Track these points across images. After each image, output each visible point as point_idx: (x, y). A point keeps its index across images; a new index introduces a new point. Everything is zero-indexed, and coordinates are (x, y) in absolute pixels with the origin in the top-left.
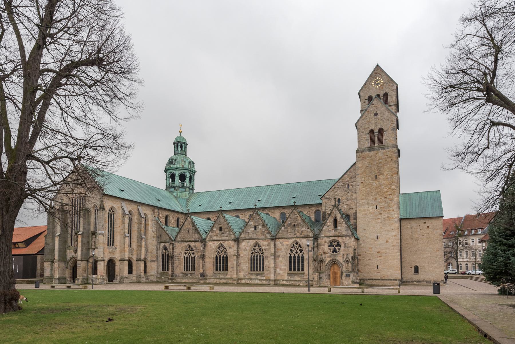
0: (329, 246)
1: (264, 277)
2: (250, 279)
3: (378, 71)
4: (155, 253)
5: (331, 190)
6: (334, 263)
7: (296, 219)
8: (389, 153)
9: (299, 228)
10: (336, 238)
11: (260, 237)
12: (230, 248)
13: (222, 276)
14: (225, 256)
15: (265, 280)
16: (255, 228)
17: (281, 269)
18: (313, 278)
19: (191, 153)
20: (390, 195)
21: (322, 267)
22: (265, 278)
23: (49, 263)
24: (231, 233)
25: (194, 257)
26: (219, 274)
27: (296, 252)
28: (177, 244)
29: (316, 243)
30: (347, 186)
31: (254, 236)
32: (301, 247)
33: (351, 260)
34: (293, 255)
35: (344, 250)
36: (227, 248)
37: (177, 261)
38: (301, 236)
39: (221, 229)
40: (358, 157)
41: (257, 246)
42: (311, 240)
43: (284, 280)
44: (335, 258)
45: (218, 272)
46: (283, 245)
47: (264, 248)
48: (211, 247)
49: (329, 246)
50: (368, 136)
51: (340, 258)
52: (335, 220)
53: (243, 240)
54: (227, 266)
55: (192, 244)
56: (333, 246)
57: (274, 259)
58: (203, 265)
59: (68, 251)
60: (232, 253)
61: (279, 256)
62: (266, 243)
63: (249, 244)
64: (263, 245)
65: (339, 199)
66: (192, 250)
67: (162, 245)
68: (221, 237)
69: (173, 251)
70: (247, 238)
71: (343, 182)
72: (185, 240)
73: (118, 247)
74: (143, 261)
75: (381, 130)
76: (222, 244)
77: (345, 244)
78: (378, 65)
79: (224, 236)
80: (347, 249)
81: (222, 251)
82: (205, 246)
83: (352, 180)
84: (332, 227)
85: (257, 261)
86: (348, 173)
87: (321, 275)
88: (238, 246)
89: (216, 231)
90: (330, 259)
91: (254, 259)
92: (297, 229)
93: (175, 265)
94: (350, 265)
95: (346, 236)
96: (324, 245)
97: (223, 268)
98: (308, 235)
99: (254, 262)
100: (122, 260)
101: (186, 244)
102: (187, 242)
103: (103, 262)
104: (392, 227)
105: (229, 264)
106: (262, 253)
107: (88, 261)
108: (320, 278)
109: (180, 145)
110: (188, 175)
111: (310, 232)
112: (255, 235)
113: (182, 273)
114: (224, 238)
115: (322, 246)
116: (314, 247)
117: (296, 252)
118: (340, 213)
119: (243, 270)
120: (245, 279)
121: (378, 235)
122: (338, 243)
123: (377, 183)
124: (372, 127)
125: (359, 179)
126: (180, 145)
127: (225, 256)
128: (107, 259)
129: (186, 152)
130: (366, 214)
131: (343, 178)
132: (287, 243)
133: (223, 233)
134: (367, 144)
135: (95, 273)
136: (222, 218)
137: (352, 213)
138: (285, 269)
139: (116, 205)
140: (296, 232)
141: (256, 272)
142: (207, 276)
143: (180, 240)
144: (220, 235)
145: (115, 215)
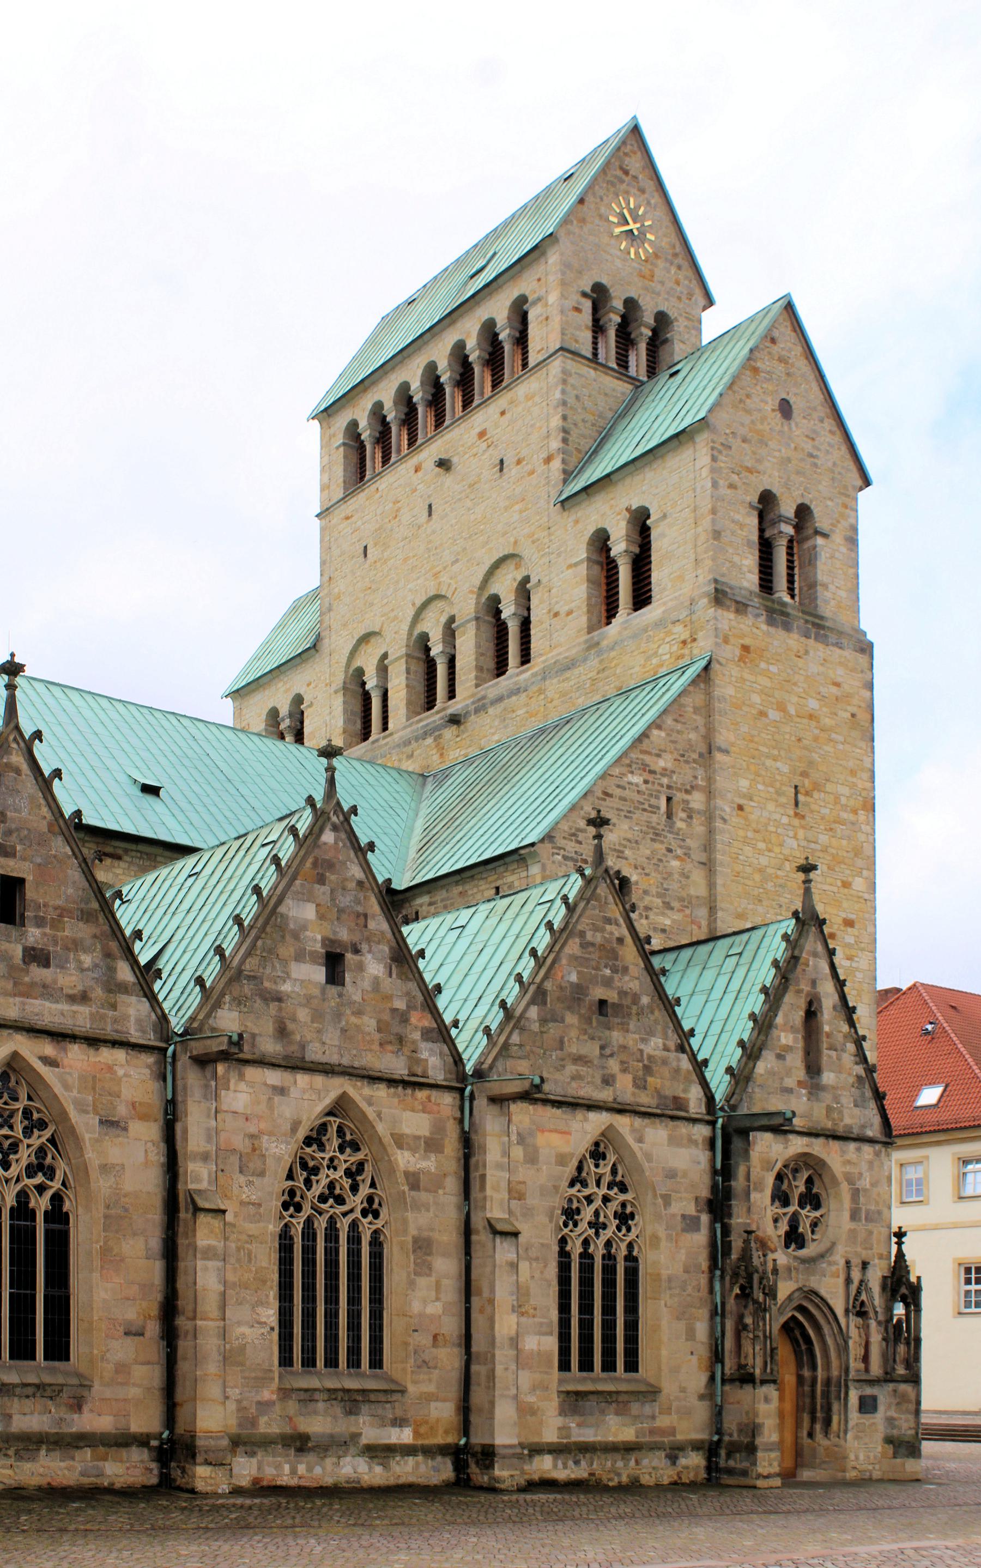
1: (399, 1422)
2: (300, 1443)
10: (817, 1147)
14: (41, 1204)
15: (409, 1450)
22: (405, 1436)
32: (623, 1188)
33: (877, 1302)
34: (575, 1248)
36: (84, 1124)
38: (646, 1100)
42: (692, 1142)
43: (536, 1450)
44: (814, 1282)
46: (532, 1159)
47: (404, 1160)
63: (286, 1110)
64: (400, 1141)
68: (27, 991)
70: (269, 1047)
71: (645, 768)
77: (856, 1193)
80: (861, 1227)
91: (309, 1252)
92: (616, 1036)
99: (309, 1288)
106: (371, 1210)
112: (332, 1036)
117: (597, 1225)
120: (241, 1442)
123: (801, 833)
127: (41, 1204)
132: (555, 1139)
140: (613, 1065)
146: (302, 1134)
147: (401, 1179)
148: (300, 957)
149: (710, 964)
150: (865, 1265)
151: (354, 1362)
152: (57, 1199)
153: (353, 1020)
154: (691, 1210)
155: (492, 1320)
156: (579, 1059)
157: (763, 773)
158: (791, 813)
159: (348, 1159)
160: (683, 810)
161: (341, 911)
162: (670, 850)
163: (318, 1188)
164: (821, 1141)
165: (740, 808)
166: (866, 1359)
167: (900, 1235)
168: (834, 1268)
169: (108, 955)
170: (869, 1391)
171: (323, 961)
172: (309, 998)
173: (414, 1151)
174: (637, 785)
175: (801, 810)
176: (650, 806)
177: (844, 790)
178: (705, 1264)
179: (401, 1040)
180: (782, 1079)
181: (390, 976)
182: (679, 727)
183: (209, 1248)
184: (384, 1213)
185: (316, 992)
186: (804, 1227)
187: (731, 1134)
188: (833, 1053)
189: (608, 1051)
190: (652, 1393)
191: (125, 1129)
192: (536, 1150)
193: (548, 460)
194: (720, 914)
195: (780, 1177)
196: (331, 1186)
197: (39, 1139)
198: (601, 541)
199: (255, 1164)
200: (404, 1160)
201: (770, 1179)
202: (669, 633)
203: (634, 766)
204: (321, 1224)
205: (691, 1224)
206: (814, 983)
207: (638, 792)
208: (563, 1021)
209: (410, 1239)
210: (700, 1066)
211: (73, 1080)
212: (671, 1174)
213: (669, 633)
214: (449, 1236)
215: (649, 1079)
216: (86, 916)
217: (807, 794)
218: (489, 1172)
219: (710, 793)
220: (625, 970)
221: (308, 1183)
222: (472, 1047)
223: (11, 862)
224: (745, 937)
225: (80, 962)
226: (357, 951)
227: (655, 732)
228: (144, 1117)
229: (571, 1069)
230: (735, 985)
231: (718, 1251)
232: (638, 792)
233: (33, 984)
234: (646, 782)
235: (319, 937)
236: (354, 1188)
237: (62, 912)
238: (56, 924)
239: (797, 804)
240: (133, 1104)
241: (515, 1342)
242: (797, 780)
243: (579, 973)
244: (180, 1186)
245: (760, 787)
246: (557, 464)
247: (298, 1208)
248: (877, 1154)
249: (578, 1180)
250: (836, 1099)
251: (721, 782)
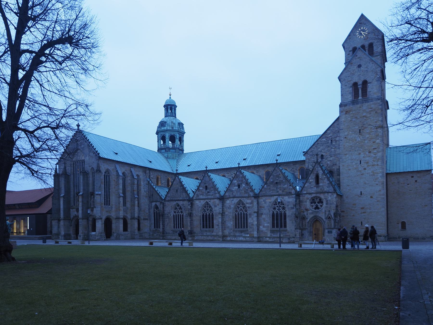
0: (311, 203)
1: (247, 234)
2: (235, 236)
3: (363, 20)
4: (148, 212)
5: (314, 147)
6: (316, 220)
7: (278, 176)
8: (373, 106)
9: (282, 186)
10: (318, 195)
11: (243, 195)
12: (215, 206)
13: (208, 234)
15: (249, 237)
16: (239, 186)
17: (264, 227)
18: (295, 235)
19: (180, 115)
20: (374, 149)
21: (304, 224)
22: (248, 235)
23: (56, 221)
24: (216, 192)
25: (183, 215)
26: (206, 231)
27: (279, 210)
28: (167, 203)
29: (298, 201)
30: (330, 141)
31: (238, 195)
32: (283, 204)
33: (333, 216)
34: (275, 213)
35: (326, 207)
36: (213, 207)
37: (167, 219)
38: (284, 193)
39: (206, 188)
40: (341, 112)
41: (241, 205)
42: (293, 197)
43: (267, 237)
44: (317, 214)
45: (205, 229)
46: (265, 203)
47: (247, 205)
48: (198, 206)
49: (311, 203)
50: (351, 89)
51: (322, 215)
52: (317, 177)
53: (228, 198)
54: (213, 223)
55: (181, 203)
56: (315, 203)
57: (258, 216)
58: (190, 223)
59: (71, 210)
60: (218, 211)
61: (262, 214)
62: (249, 201)
63: (233, 202)
64: (247, 203)
65: (322, 156)
66: (181, 208)
67: (154, 204)
68: (208, 195)
69: (164, 210)
70: (231, 196)
71: (326, 137)
72: (174, 199)
73: (113, 206)
74: (136, 219)
75: (365, 83)
76: (208, 203)
77: (327, 201)
78: (362, 15)
79: (209, 195)
81: (208, 210)
82: (192, 205)
83: (335, 135)
84: (314, 183)
85: (241, 218)
86: (331, 128)
87: (304, 232)
88: (223, 204)
89: (202, 190)
90: (312, 216)
92: (279, 186)
93: (166, 223)
94: (332, 222)
95: (328, 192)
96: (306, 202)
97: (209, 225)
98: (290, 193)
100: (118, 218)
101: (175, 203)
102: (175, 201)
103: (100, 220)
104: (377, 182)
105: (215, 222)
106: (246, 211)
107: (88, 219)
108: (302, 235)
109: (170, 108)
110: (178, 136)
111: (292, 189)
112: (239, 194)
113: (172, 231)
114: (209, 197)
115: (304, 203)
116: (296, 204)
117: (279, 210)
118: (322, 169)
119: (228, 227)
121: (362, 190)
122: (320, 199)
123: (361, 137)
124: (355, 79)
125: (342, 134)
126: (170, 108)
127: (211, 214)
128: (104, 218)
129: (175, 114)
130: (350, 170)
131: (326, 134)
132: (269, 200)
133: (208, 192)
134: (350, 98)
135: (94, 230)
136: (207, 177)
137: (336, 169)
138: (268, 227)
139: (111, 167)
141: (240, 229)
142: (194, 233)
143: (169, 199)
145: (110, 177)
148: (235, 186)
150: (329, 211)
151: (244, 227)
154: (293, 206)
170: (330, 230)
190: (286, 231)
200: (247, 205)
204: (240, 213)
205: (292, 208)
212: (289, 202)
239: (360, 132)
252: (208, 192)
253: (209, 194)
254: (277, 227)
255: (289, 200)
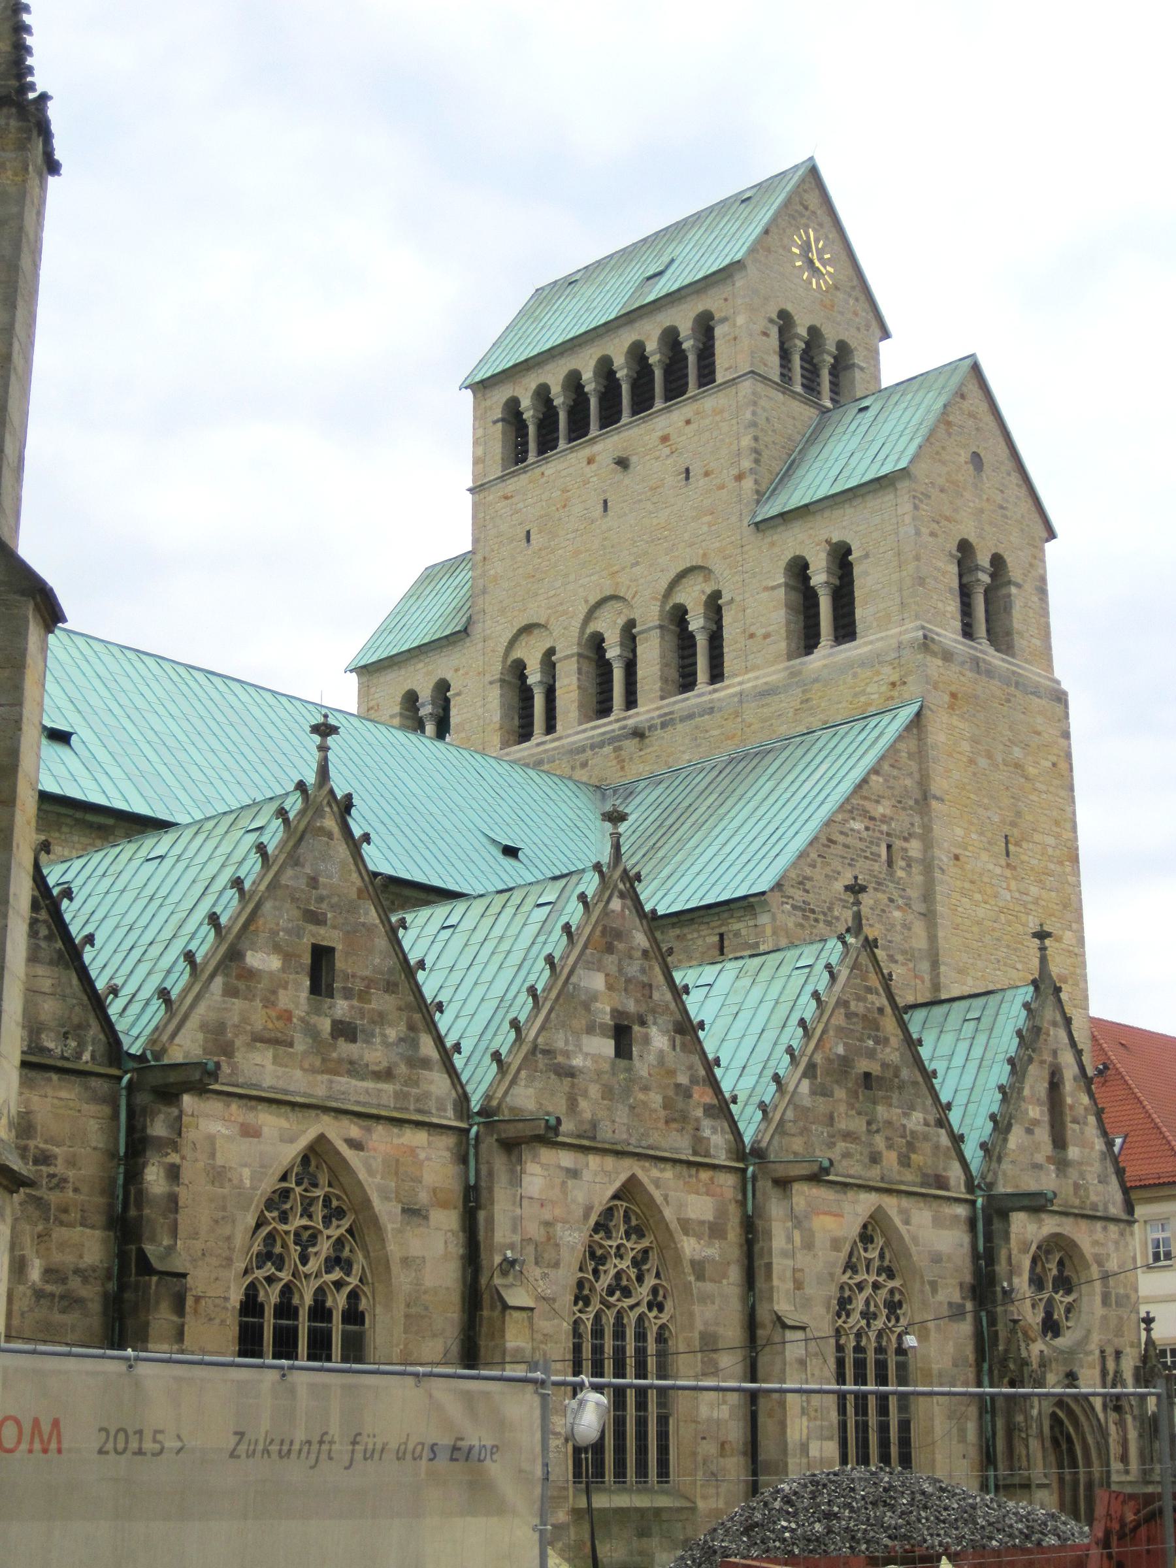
7: (871, 1023)
12: (413, 1213)
14: (338, 1302)
46: (809, 1245)
47: (690, 1247)
48: (218, 1175)
68: (331, 1068)
79: (354, 1069)
84: (1043, 1135)
92: (881, 1111)
98: (941, 1182)
112: (622, 1115)
114: (356, 1091)
123: (1013, 884)
127: (338, 1302)
133: (345, 1031)
136: (342, 850)
144: (318, 1044)
146: (593, 1219)
147: (688, 1269)
148: (590, 1030)
149: (947, 1028)
152: (354, 1296)
153: (641, 1096)
155: (783, 1425)
156: (848, 1136)
157: (976, 821)
158: (1003, 863)
159: (633, 1246)
160: (903, 859)
161: (628, 981)
162: (891, 900)
163: (605, 1281)
164: (1071, 1220)
165: (957, 858)
166: (1124, 1458)
167: (1148, 1320)
168: (1090, 1358)
169: (412, 1027)
171: (611, 1033)
172: (599, 1073)
173: (699, 1237)
174: (859, 832)
175: (1012, 861)
176: (872, 853)
177: (1051, 841)
178: (971, 1357)
179: (684, 1118)
180: (1032, 1154)
181: (674, 1048)
182: (895, 772)
183: (518, 1350)
184: (669, 1305)
185: (606, 1067)
186: (1059, 1314)
187: (990, 1215)
188: (1076, 1127)
189: (874, 1127)
191: (426, 1218)
192: (811, 1233)
193: (739, 477)
194: (943, 969)
195: (1034, 1261)
196: (618, 1276)
197: (337, 1230)
198: (799, 569)
199: (549, 1255)
201: (1027, 1264)
202: (878, 673)
203: (855, 812)
206: (1055, 1053)
207: (861, 839)
208: (832, 1095)
209: (697, 1335)
210: (957, 1140)
211: (377, 1164)
212: (937, 1259)
213: (878, 673)
214: (732, 1332)
215: (913, 1156)
216: (390, 987)
217: (1017, 844)
218: (775, 1261)
219: (928, 842)
220: (886, 1041)
221: (596, 1272)
222: (750, 1126)
223: (322, 931)
224: (981, 1001)
225: (384, 1036)
226: (643, 1023)
227: (874, 777)
228: (444, 1205)
229: (841, 1145)
230: (977, 1052)
231: (984, 1344)
232: (861, 839)
233: (340, 1061)
234: (867, 829)
235: (608, 1009)
236: (640, 1279)
237: (370, 982)
238: (363, 996)
239: (1008, 854)
240: (434, 1191)
241: (804, 1448)
242: (1007, 830)
243: (845, 1044)
244: (483, 1281)
245: (974, 836)
246: (748, 484)
247: (587, 1303)
248: (1122, 1234)
249: (850, 1266)
250: (1082, 1175)
251: (938, 830)
252: (345, 1031)
253: (345, 1049)
254: (864, 1460)
255: (936, 1238)
